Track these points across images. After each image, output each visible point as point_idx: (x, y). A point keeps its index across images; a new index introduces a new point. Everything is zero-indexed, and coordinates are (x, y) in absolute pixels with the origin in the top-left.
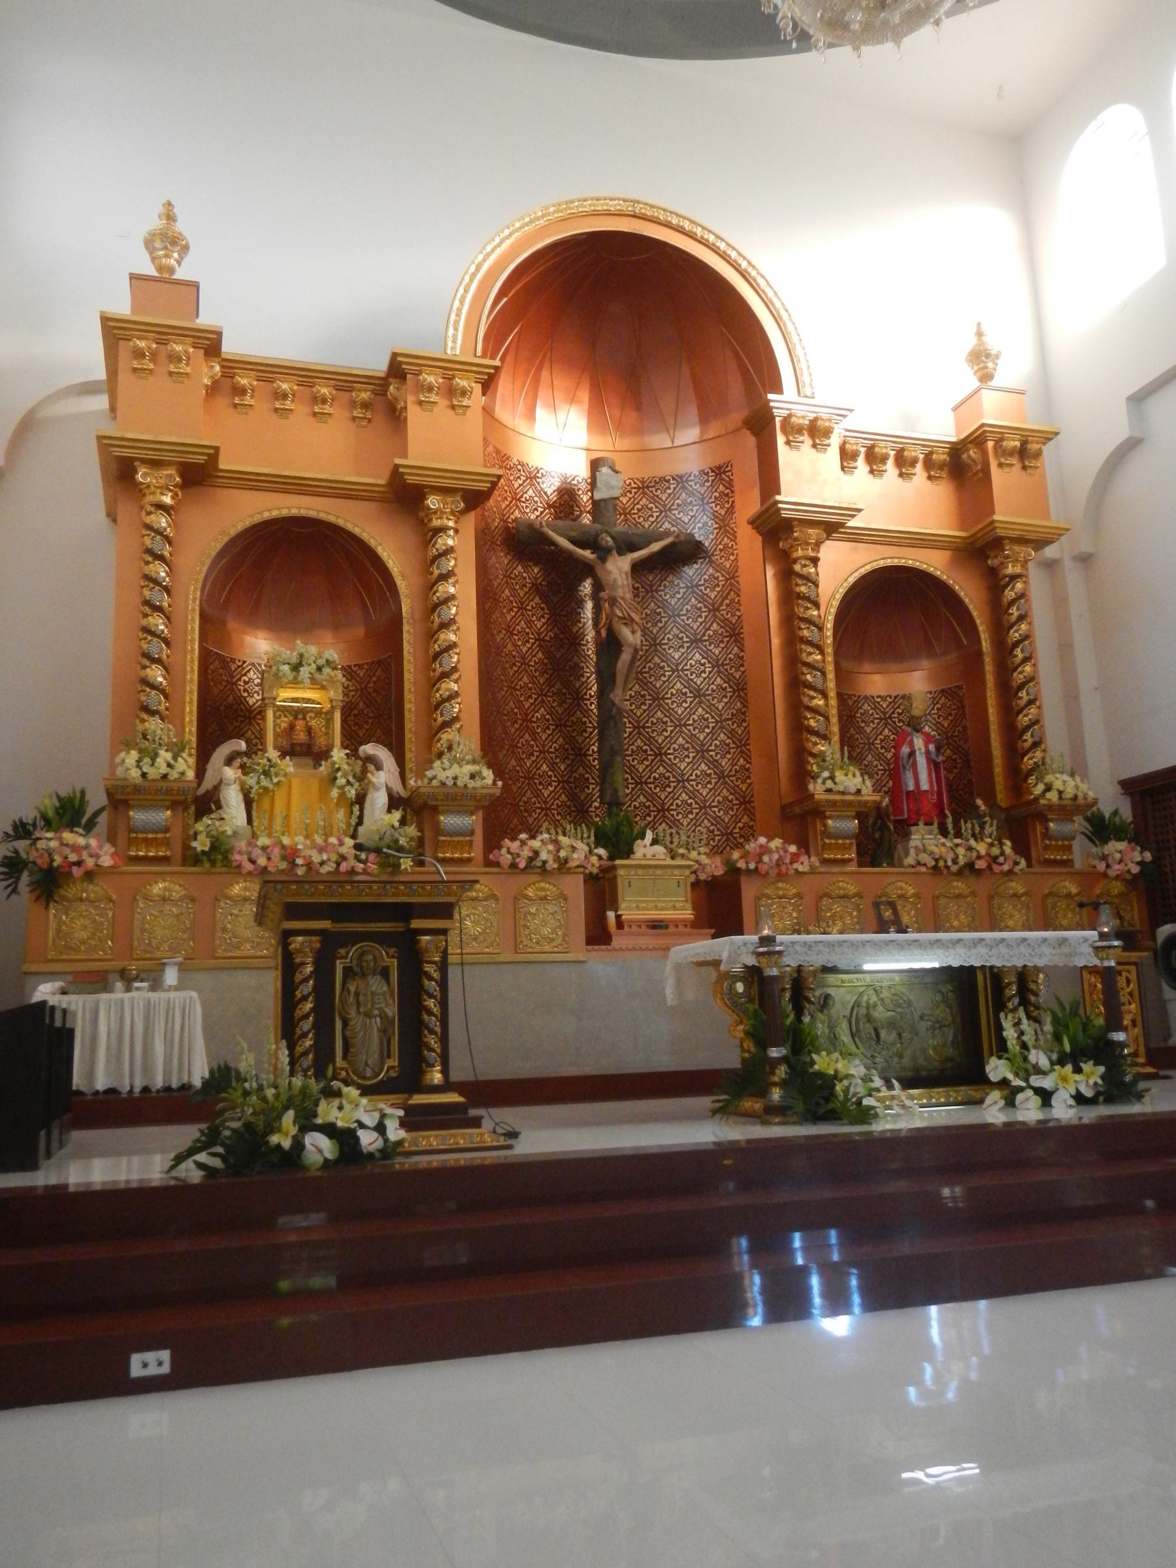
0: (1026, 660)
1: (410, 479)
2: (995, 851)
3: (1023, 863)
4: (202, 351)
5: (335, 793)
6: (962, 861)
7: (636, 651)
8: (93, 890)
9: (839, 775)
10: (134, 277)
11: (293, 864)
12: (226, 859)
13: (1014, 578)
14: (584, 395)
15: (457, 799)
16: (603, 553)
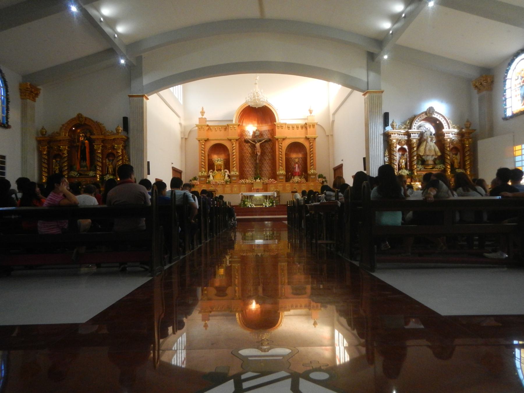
0: (311, 154)
1: (229, 139)
2: (301, 180)
3: (305, 181)
4: (206, 127)
5: (222, 175)
6: (296, 181)
7: (259, 155)
8: (197, 187)
9: (280, 172)
10: (199, 118)
11: (216, 184)
12: (210, 183)
13: (311, 143)
14: (256, 119)
15: (233, 176)
16: (256, 143)
